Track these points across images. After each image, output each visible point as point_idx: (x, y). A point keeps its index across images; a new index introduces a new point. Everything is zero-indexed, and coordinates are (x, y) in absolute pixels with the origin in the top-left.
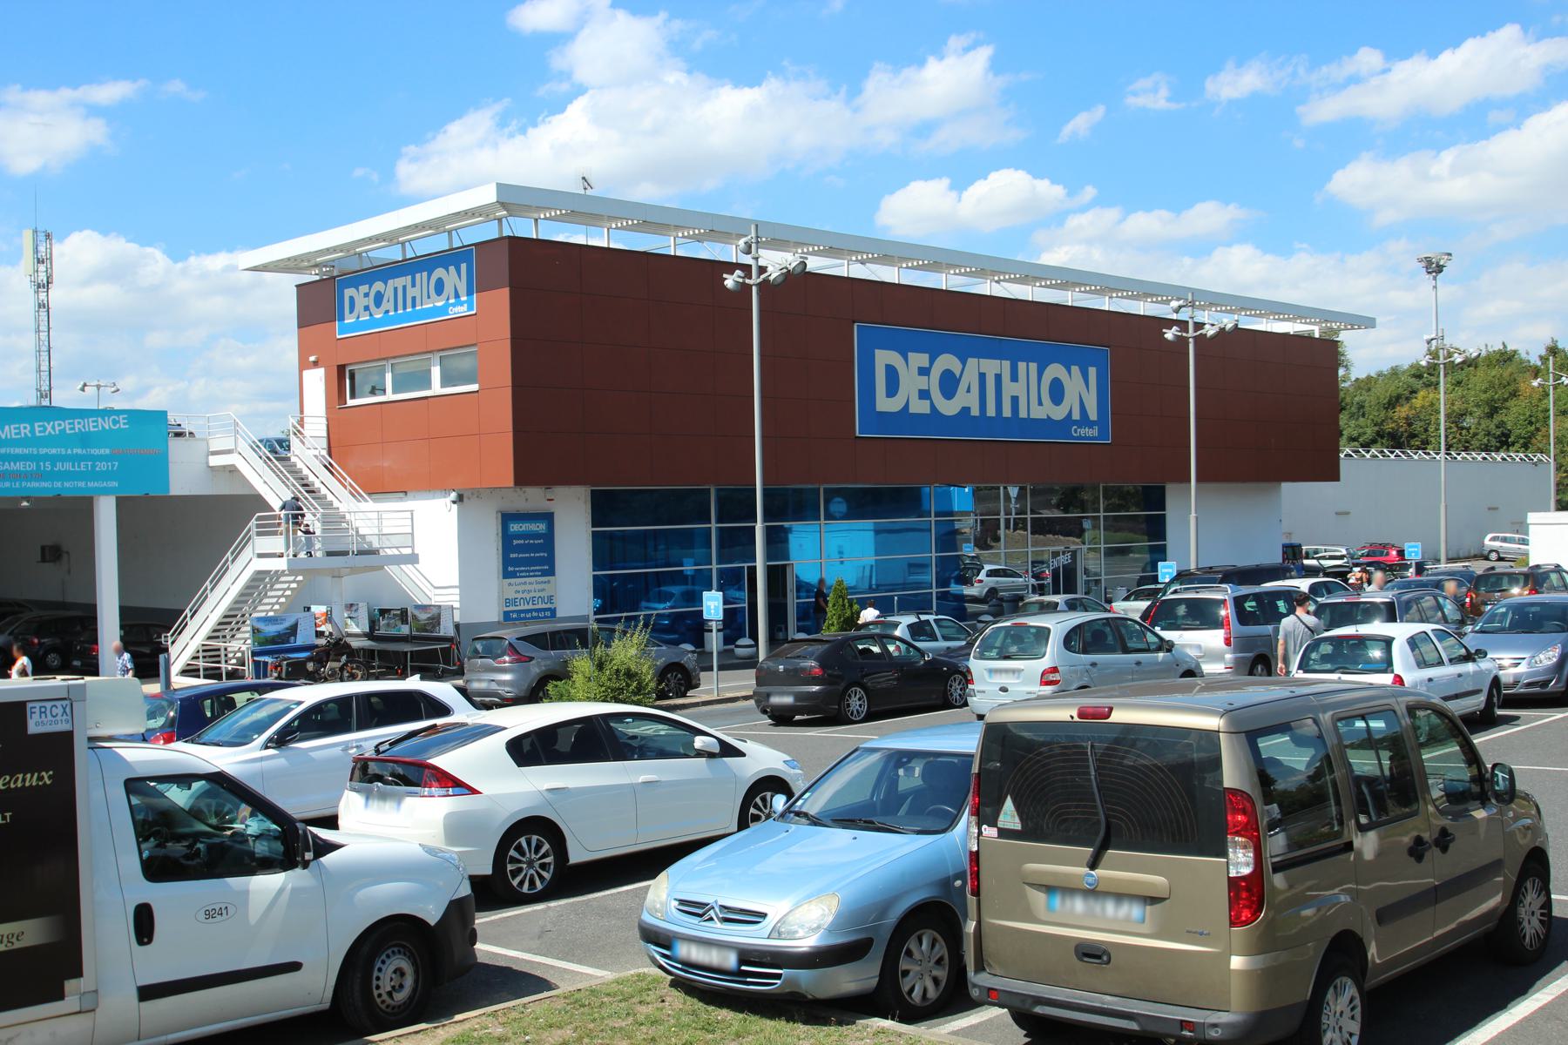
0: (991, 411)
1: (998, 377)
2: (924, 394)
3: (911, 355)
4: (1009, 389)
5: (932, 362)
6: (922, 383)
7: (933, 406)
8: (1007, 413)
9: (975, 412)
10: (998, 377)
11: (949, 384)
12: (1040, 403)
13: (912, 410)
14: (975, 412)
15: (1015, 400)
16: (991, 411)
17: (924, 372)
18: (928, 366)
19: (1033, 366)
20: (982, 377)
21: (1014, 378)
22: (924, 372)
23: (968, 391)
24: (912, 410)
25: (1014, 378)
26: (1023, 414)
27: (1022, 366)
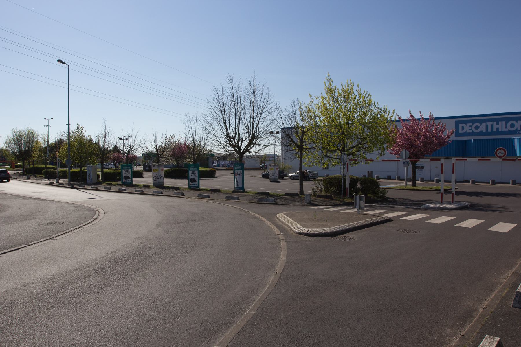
0: (489, 130)
1: (492, 126)
2: (470, 130)
3: (467, 124)
4: (495, 126)
5: (472, 125)
6: (470, 128)
7: (472, 131)
8: (495, 130)
9: (484, 131)
10: (492, 126)
11: (477, 128)
12: (506, 127)
13: (467, 132)
14: (484, 131)
15: (497, 129)
16: (489, 130)
17: (470, 126)
18: (471, 125)
19: (504, 123)
20: (487, 126)
21: (497, 124)
22: (470, 126)
23: (483, 128)
24: (467, 132)
25: (497, 124)
26: (500, 130)
27: (500, 123)
